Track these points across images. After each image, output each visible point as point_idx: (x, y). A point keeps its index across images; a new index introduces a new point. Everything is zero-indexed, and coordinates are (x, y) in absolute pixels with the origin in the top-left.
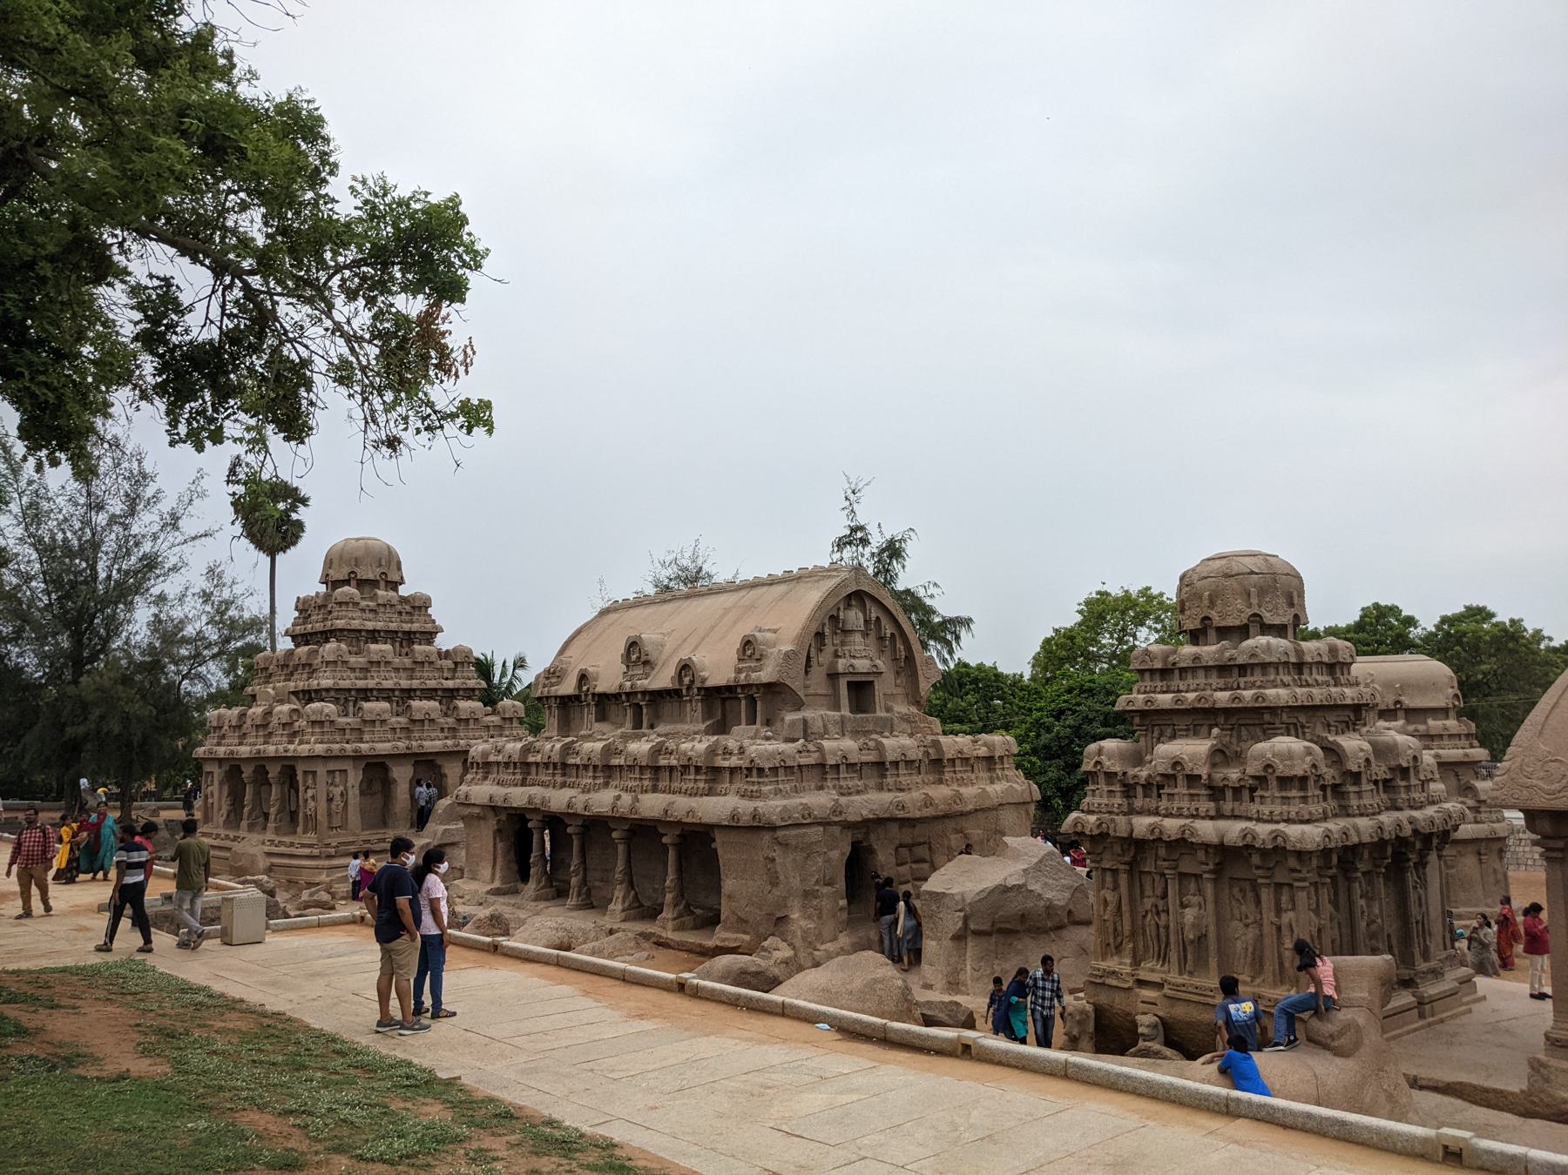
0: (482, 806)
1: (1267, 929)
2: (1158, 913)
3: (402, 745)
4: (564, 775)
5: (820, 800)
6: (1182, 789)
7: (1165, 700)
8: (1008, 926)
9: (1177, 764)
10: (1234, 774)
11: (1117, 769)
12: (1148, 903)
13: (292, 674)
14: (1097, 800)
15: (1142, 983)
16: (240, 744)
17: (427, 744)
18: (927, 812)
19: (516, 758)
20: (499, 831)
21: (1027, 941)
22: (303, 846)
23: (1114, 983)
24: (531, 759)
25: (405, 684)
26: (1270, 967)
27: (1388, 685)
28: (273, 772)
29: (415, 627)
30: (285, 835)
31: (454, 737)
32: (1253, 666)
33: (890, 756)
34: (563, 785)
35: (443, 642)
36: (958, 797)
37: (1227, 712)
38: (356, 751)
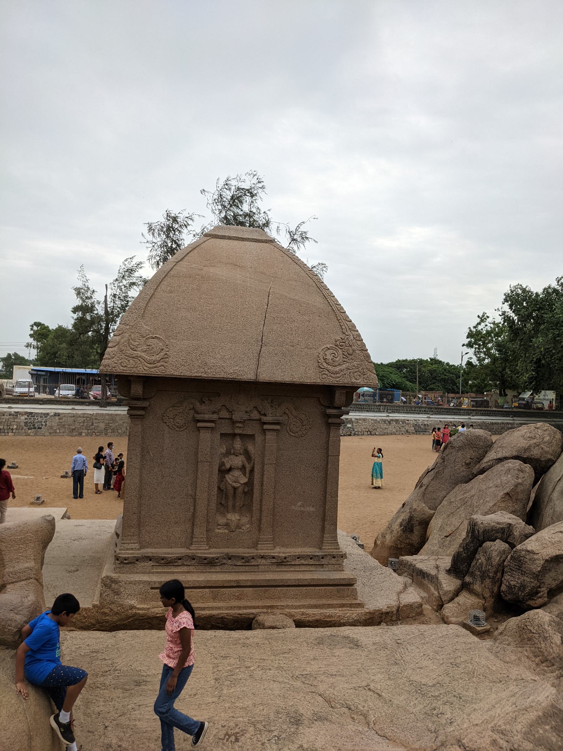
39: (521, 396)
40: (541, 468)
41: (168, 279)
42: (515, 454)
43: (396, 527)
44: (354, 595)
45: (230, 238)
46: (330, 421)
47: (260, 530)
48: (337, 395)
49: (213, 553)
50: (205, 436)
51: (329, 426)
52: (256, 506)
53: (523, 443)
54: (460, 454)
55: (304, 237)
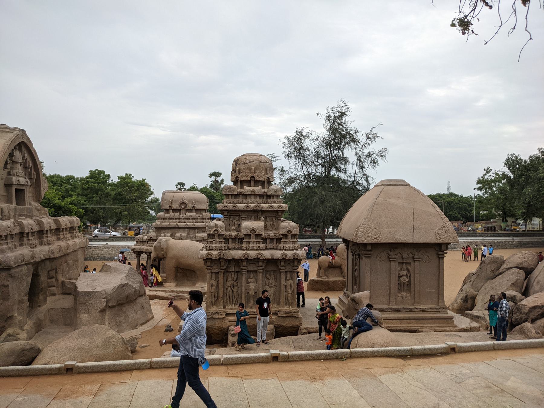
1: (283, 287)
2: (233, 287)
5: (24, 251)
6: (253, 239)
7: (241, 206)
8: (122, 302)
9: (253, 230)
10: (272, 234)
11: (224, 232)
12: (229, 284)
14: (214, 245)
15: (228, 315)
18: (60, 254)
21: (127, 307)
23: (217, 316)
26: (282, 300)
27: (191, 201)
32: (273, 196)
33: (46, 228)
36: (68, 247)
37: (263, 212)
39: (517, 222)
40: (528, 272)
41: (375, 206)
42: (515, 265)
43: (459, 300)
44: (453, 322)
45: (393, 185)
46: (440, 256)
47: (414, 299)
48: (443, 246)
49: (398, 307)
50: (392, 263)
51: (439, 258)
52: (412, 290)
53: (519, 261)
54: (489, 266)
55: (375, 136)
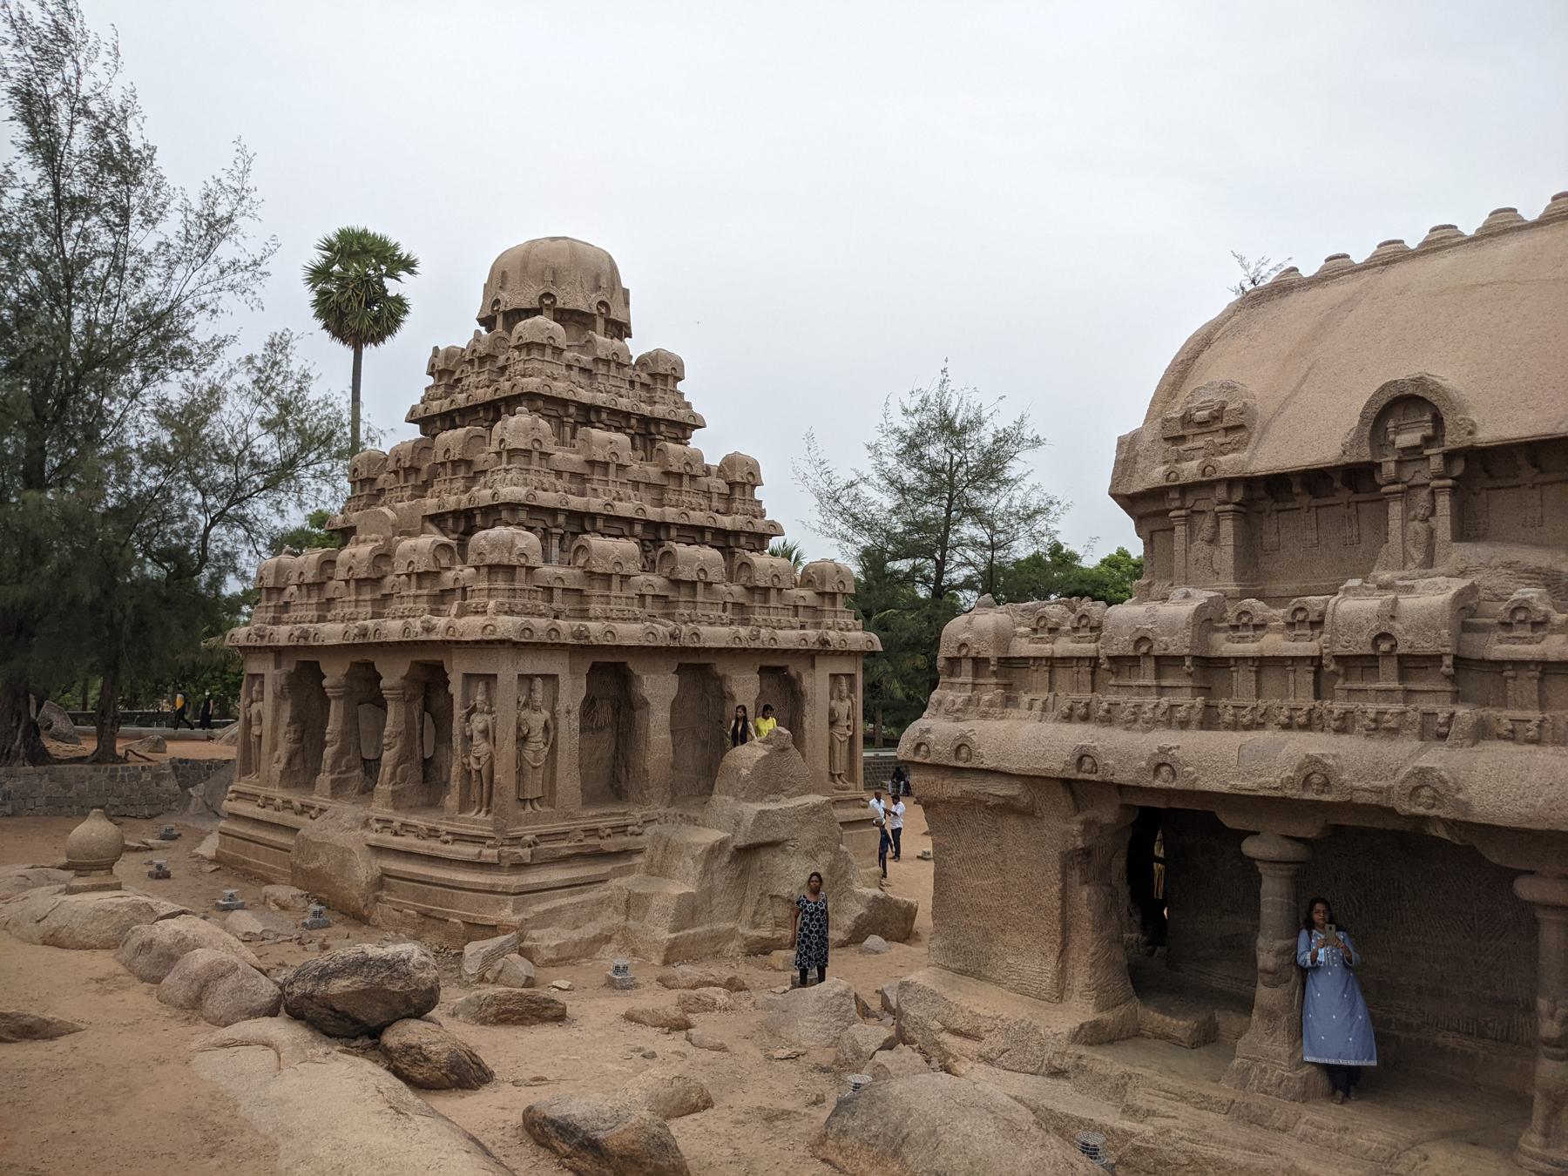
0: (1030, 780)
3: (663, 628)
4: (1458, 697)
13: (426, 485)
16: (322, 619)
17: (705, 630)
19: (1178, 644)
20: (1087, 852)
22: (459, 838)
24: (1226, 646)
25: (653, 513)
28: (392, 676)
29: (660, 410)
30: (412, 809)
31: (745, 622)
34: (1482, 732)
35: (710, 447)
38: (578, 635)
